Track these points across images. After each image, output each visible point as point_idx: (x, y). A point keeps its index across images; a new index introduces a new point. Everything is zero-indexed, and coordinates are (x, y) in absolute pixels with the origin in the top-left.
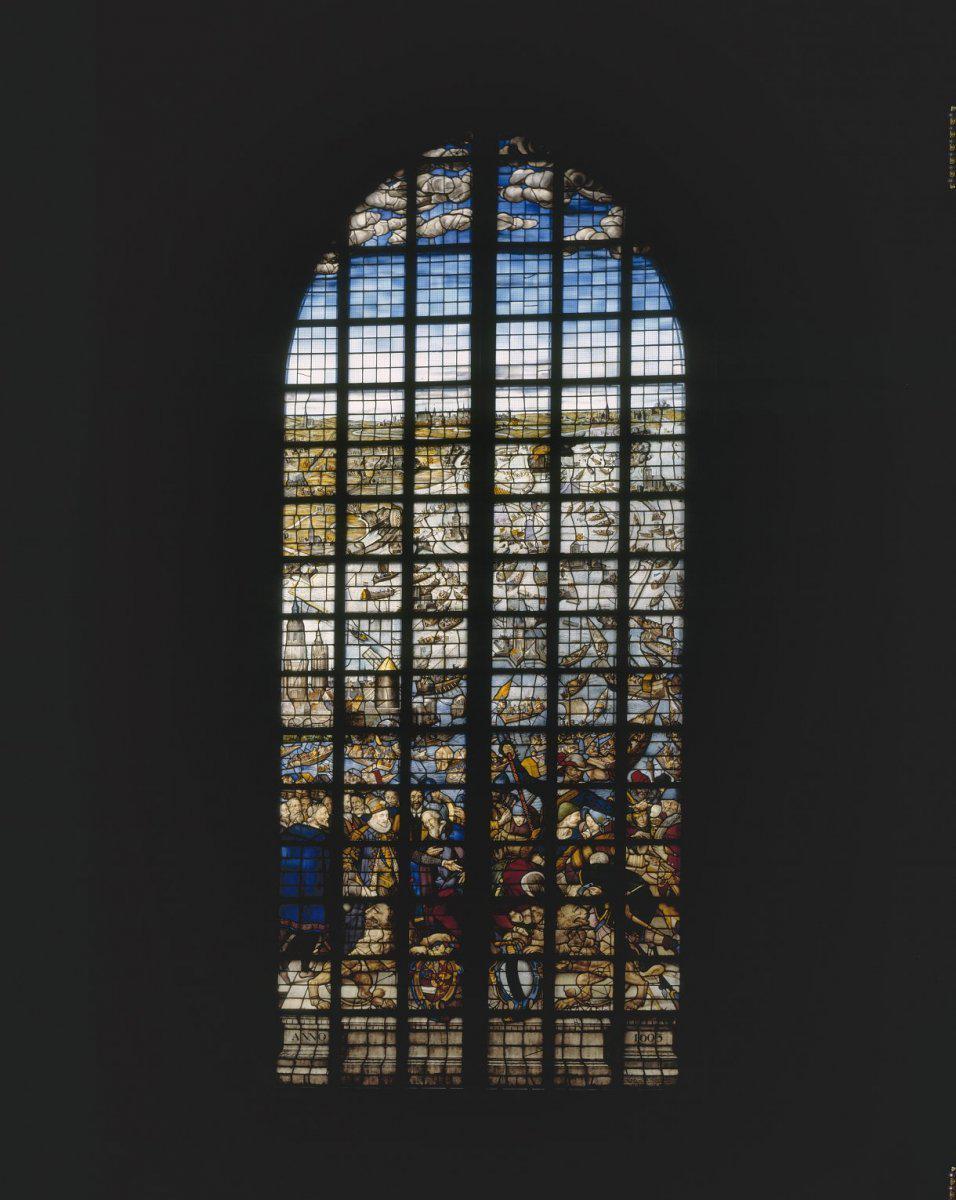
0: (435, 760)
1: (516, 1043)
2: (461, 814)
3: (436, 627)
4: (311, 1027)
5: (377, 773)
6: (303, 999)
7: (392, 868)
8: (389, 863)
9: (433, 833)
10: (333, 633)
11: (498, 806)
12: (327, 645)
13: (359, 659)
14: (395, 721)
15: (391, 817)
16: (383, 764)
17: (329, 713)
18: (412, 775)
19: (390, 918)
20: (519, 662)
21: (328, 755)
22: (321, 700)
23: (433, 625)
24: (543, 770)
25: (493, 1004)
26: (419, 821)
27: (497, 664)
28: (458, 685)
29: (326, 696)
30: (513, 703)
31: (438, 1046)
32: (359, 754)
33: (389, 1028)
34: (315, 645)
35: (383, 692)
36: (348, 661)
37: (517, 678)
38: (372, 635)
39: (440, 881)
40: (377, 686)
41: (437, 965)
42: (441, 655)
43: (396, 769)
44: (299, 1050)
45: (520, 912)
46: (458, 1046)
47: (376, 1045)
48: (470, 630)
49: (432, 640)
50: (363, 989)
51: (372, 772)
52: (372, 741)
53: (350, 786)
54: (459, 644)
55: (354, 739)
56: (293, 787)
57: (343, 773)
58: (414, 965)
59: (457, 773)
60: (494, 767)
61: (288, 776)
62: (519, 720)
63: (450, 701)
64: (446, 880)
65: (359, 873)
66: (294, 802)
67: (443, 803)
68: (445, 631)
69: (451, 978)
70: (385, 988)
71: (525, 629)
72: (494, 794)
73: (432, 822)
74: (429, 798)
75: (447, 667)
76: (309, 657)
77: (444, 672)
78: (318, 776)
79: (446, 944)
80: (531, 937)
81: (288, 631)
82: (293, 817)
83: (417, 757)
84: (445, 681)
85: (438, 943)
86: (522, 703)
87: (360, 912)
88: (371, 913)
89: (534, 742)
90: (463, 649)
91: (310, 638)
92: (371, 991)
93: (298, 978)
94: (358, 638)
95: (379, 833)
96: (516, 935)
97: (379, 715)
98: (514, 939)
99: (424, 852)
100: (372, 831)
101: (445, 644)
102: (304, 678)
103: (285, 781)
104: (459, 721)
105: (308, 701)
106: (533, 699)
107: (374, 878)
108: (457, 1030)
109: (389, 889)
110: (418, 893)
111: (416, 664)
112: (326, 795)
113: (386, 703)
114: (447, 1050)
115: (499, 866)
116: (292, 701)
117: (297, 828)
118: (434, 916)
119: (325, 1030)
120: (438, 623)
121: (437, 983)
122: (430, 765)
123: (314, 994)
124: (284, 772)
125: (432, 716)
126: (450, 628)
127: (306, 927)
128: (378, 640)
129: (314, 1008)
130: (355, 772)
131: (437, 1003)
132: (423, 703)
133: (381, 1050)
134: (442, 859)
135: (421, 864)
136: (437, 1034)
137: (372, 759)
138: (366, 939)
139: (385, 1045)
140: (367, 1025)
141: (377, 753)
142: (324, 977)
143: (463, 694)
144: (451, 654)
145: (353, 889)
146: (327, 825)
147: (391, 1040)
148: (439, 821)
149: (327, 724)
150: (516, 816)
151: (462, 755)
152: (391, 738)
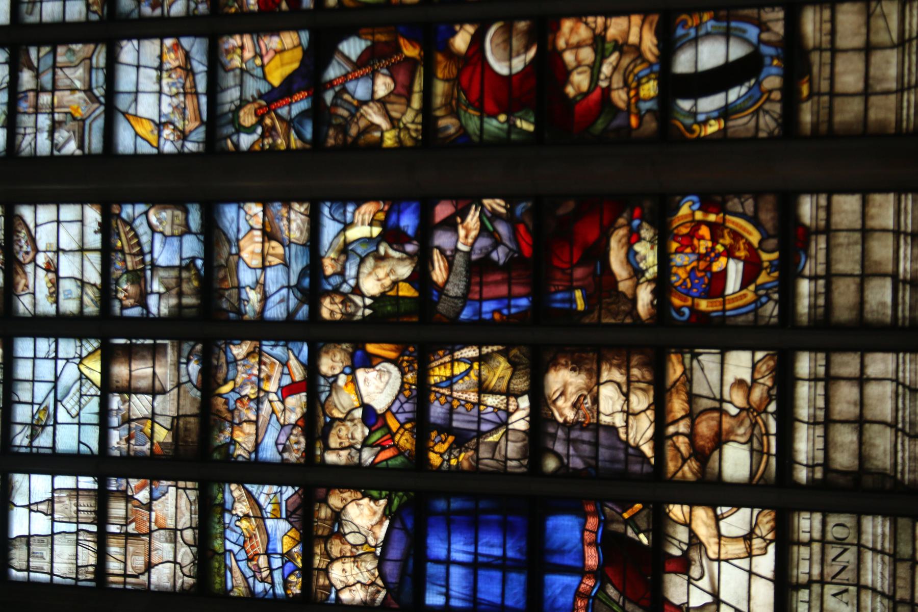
0: (264, 268)
1: (861, 66)
2: (368, 209)
3: (30, 269)
4: (817, 557)
5: (287, 391)
6: (751, 573)
7: (471, 360)
8: (460, 368)
9: (405, 270)
10: (34, 477)
11: (353, 131)
12: (53, 490)
13: (79, 424)
14: (190, 353)
15: (369, 362)
16: (269, 378)
17: (172, 490)
18: (291, 315)
19: (576, 367)
20: (94, 99)
21: (249, 494)
22: (149, 507)
23: (25, 273)
24: (289, 39)
25: (767, 123)
26: (379, 300)
27: (96, 143)
28: (130, 223)
29: (143, 496)
30: (166, 109)
31: (865, 254)
32: (249, 429)
33: (821, 371)
34: (52, 514)
35: (139, 378)
36: (83, 448)
37: (123, 102)
38: (38, 400)
39: (499, 255)
40: (129, 390)
41: (678, 259)
42: (77, 258)
43: (279, 351)
44: (874, 590)
45: (565, 74)
46: (865, 204)
47: (862, 403)
48: (35, 201)
49: (51, 276)
50: (731, 431)
51: (283, 402)
52: (227, 403)
53: (309, 450)
54: (58, 222)
55: (224, 437)
56: (307, 572)
57: (284, 463)
58: (678, 310)
59: (289, 220)
60: (281, 142)
61: (286, 584)
62: (197, 94)
63: (158, 237)
64: (497, 242)
65: (480, 434)
66: (337, 573)
67: (346, 250)
68: (36, 251)
69: (709, 224)
70: (729, 379)
71: (39, 90)
72: (331, 142)
73: (381, 273)
74: (336, 280)
75: (98, 245)
76: (73, 528)
77: (107, 251)
78: (287, 519)
79: (633, 237)
80: (621, 47)
81: (28, 569)
82: (365, 578)
83: (257, 307)
84: (122, 251)
85: (631, 257)
86: (166, 89)
87: (560, 433)
88: (565, 411)
89: (237, 62)
90: (69, 212)
91: (41, 525)
92: (734, 411)
93: (705, 583)
94: (44, 427)
95: (403, 383)
96: (617, 81)
97: (179, 385)
98: (626, 85)
99: (441, 289)
100: (397, 404)
101: (58, 250)
102: (112, 541)
103: (297, 590)
104: (195, 219)
105: (150, 533)
106: (160, 68)
107: (491, 400)
108: (828, 208)
109: (514, 365)
110: (524, 302)
111: (91, 309)
112: (325, 501)
113: (159, 371)
114: (874, 230)
115: (473, 124)
116: (149, 566)
117: (389, 568)
118: (573, 266)
119: (824, 524)
120: (22, 265)
121: (718, 255)
122: (275, 278)
123: (739, 548)
124: (280, 590)
125: (185, 275)
126: (33, 240)
127: (592, 558)
128: (52, 385)
129: (772, 549)
130: (283, 439)
131: (765, 257)
132: (160, 295)
133: (873, 390)
134: (456, 250)
135: (465, 298)
136: (838, 254)
137: (258, 401)
138: (619, 421)
139: (862, 380)
140: (813, 423)
141: (249, 391)
142: (702, 517)
143: (146, 213)
144: (77, 238)
145: (513, 449)
146: (383, 502)
147: (847, 364)
148: (380, 259)
149: (193, 495)
150: (373, 92)
151: (256, 209)
152: (223, 360)
